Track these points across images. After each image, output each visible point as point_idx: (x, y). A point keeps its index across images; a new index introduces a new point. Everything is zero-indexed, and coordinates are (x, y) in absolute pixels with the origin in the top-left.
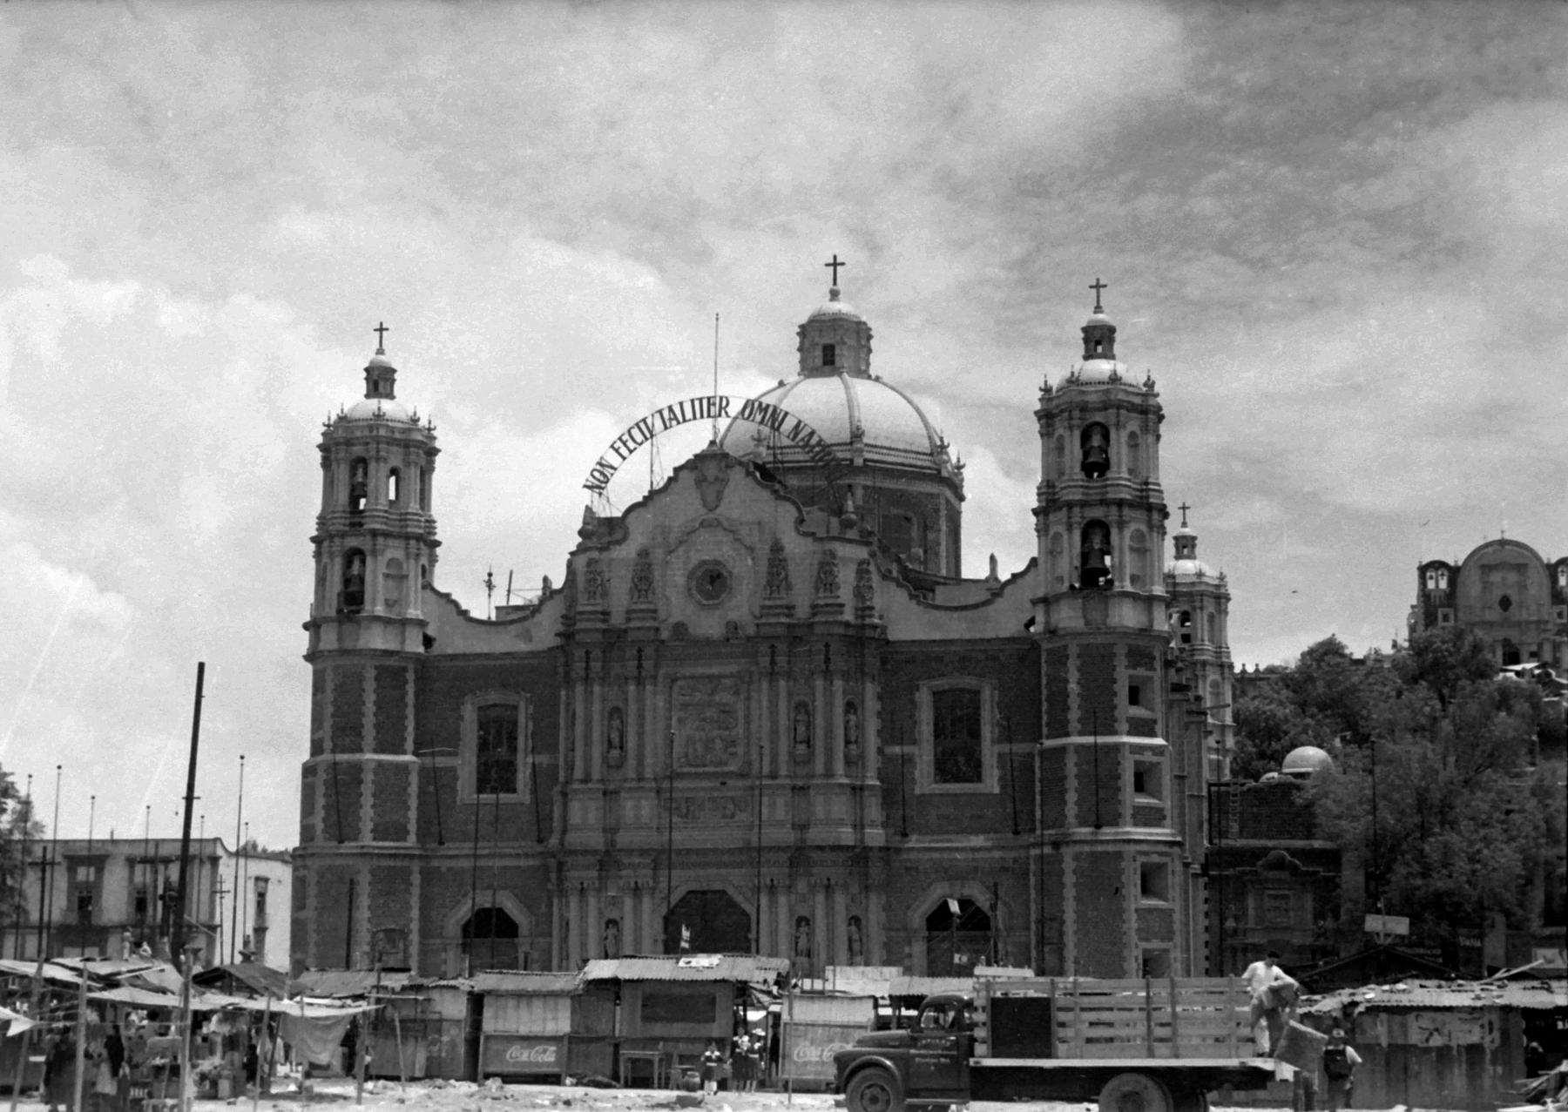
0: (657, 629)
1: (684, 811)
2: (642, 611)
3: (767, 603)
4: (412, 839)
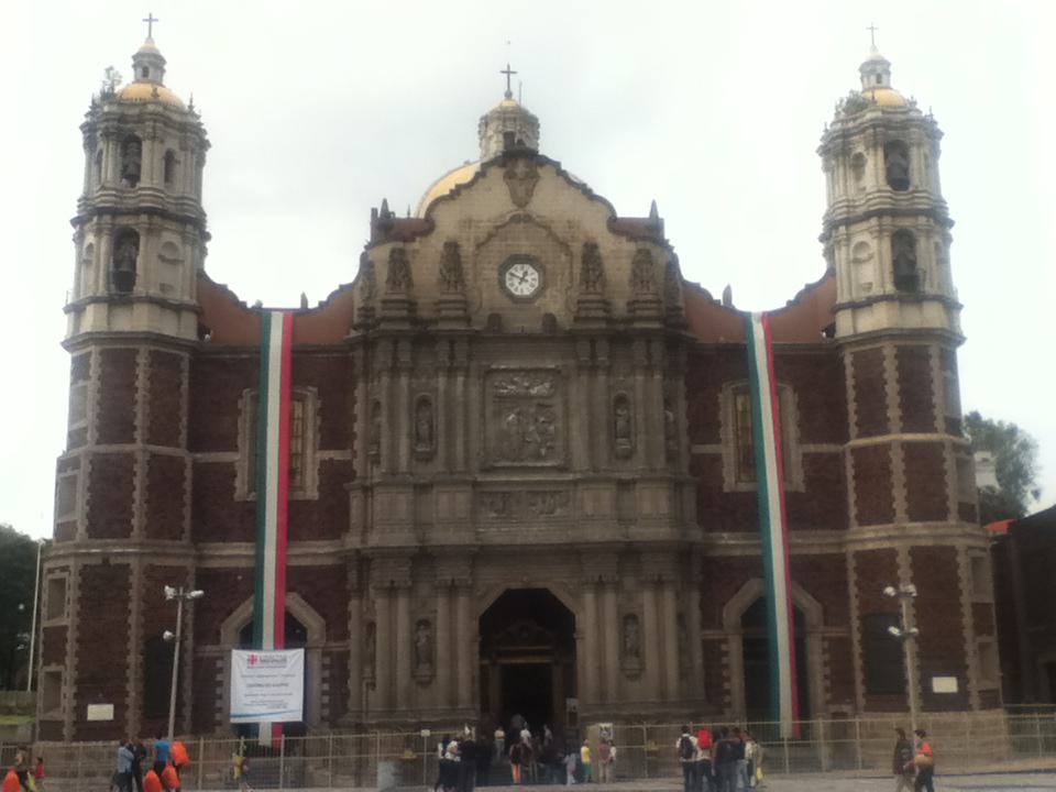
0: (468, 320)
1: (500, 505)
2: (450, 302)
3: (584, 298)
4: (186, 540)
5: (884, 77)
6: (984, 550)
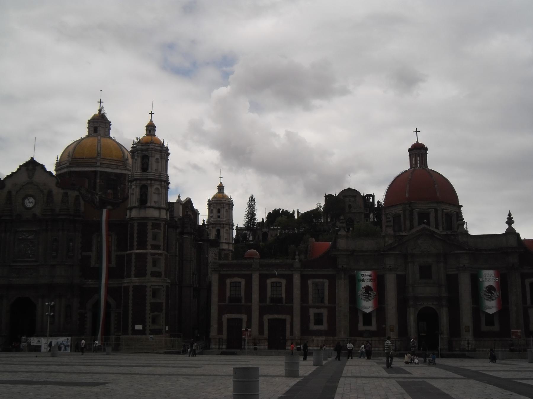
5: (152, 131)
6: (159, 286)
